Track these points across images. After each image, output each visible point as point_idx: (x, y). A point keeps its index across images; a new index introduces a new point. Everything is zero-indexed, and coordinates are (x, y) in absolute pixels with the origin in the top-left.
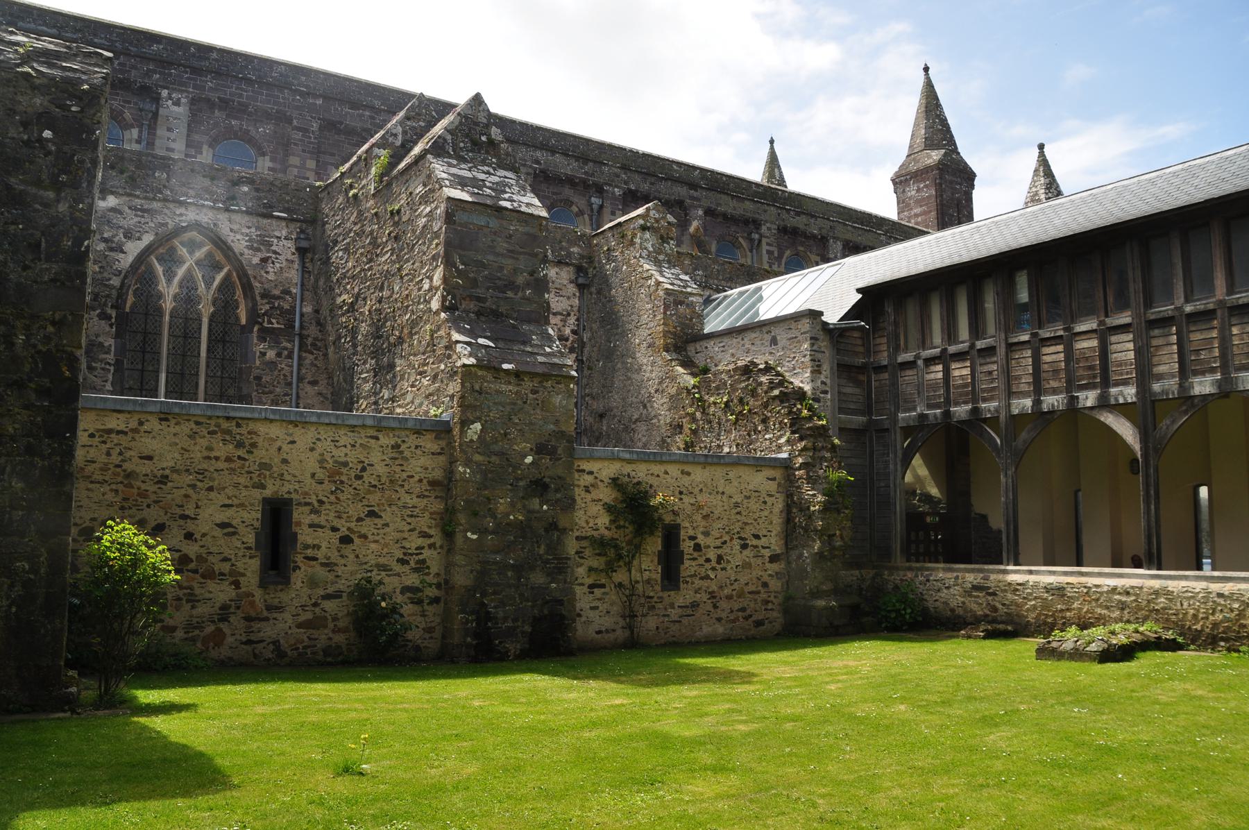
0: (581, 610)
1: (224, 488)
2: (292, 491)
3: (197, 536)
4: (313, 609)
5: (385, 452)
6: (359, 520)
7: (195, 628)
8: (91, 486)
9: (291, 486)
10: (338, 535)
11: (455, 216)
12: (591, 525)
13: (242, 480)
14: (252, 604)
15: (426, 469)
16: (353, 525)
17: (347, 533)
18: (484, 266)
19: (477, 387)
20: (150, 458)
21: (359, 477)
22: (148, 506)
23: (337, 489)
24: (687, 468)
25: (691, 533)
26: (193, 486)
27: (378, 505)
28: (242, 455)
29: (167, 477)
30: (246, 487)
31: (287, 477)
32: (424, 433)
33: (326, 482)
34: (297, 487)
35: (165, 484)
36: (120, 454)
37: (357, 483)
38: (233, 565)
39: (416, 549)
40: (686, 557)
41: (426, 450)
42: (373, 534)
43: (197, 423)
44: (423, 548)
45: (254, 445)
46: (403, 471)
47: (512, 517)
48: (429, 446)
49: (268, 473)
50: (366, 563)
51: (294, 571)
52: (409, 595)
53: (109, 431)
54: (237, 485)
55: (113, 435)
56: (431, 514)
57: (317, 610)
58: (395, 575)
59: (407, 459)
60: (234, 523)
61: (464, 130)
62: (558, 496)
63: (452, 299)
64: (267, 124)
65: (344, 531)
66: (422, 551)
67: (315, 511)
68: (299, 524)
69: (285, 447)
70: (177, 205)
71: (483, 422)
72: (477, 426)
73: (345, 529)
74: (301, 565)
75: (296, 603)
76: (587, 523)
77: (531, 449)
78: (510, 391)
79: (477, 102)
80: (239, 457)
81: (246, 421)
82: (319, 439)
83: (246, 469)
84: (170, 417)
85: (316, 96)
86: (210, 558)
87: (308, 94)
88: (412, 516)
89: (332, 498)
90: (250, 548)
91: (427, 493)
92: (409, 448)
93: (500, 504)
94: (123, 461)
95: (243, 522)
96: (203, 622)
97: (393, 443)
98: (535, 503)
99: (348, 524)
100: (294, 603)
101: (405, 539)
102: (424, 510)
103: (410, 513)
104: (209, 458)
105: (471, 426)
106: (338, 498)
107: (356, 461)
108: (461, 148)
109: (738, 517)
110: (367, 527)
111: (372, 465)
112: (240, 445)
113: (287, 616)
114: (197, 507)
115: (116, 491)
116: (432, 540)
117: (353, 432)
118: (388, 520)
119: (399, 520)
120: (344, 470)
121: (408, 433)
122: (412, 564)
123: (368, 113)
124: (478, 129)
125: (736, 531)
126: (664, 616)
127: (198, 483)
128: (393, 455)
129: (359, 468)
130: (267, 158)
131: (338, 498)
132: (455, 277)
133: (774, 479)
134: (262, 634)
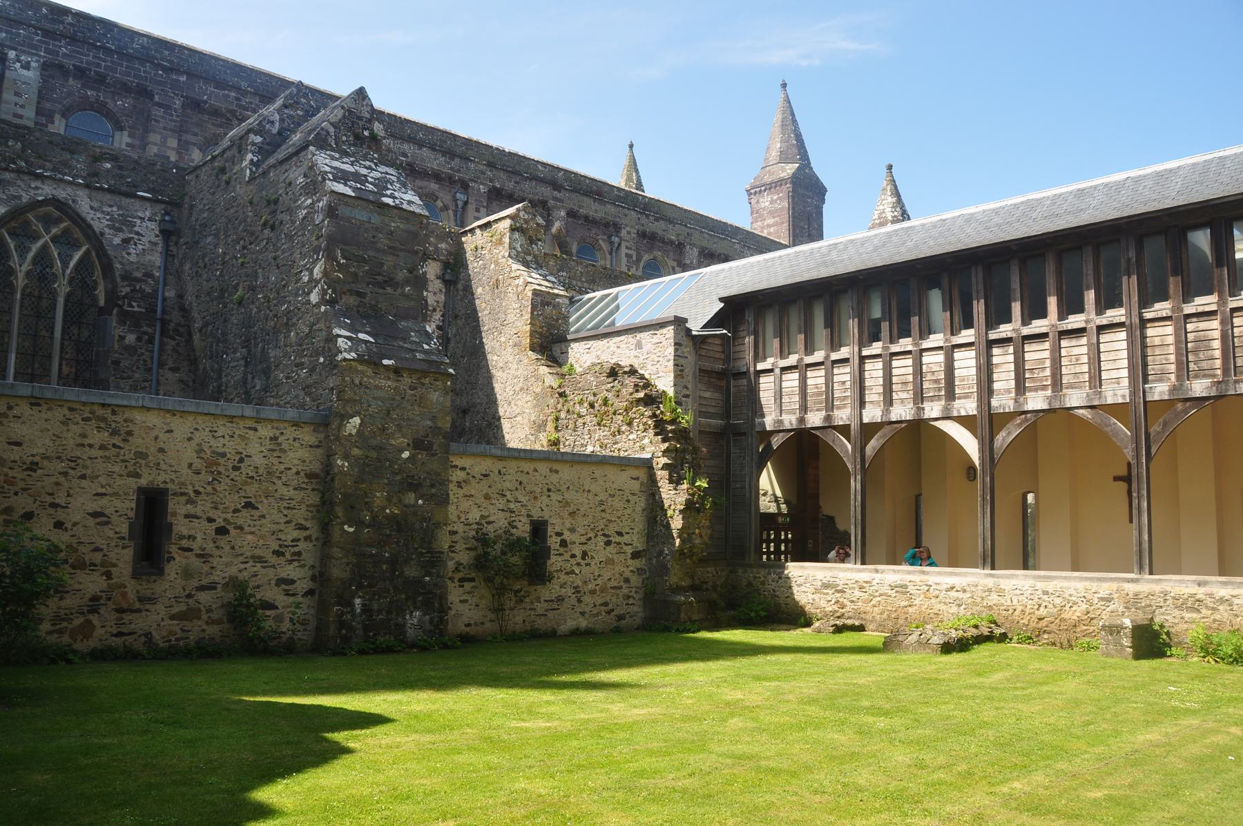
0: (452, 603)
1: (97, 477)
2: (168, 480)
3: (68, 525)
4: (187, 600)
5: (263, 444)
6: (236, 511)
7: (63, 620)
9: (167, 476)
10: (214, 526)
11: (337, 210)
12: (461, 520)
13: (116, 469)
14: (124, 595)
15: (304, 461)
16: (229, 516)
17: (223, 524)
18: (364, 261)
19: (357, 382)
20: (19, 444)
21: (235, 468)
23: (214, 479)
24: (555, 466)
25: (558, 529)
26: (65, 474)
27: (255, 496)
28: (118, 444)
29: (37, 464)
30: (121, 475)
31: (163, 466)
32: (303, 425)
33: (203, 472)
34: (172, 477)
35: (35, 471)
37: (234, 474)
38: (105, 555)
39: (292, 541)
40: (552, 552)
41: (304, 443)
42: (249, 526)
43: (71, 409)
44: (299, 540)
45: (130, 433)
46: (280, 463)
47: (388, 511)
48: (307, 438)
49: (143, 462)
50: (241, 555)
51: (168, 561)
52: (284, 587)
54: (110, 474)
56: (307, 506)
57: (191, 601)
58: (271, 567)
60: (107, 512)
61: (347, 124)
62: (433, 491)
63: (332, 293)
64: (126, 97)
65: (220, 522)
66: (298, 544)
67: (190, 501)
68: (174, 514)
69: (163, 436)
70: (32, 178)
71: (362, 416)
72: (357, 420)
73: (221, 520)
74: (175, 556)
75: (168, 594)
76: (459, 518)
77: (408, 444)
78: (389, 386)
80: (114, 446)
81: (123, 409)
82: (197, 429)
83: (121, 458)
84: (41, 402)
86: (81, 548)
87: (171, 70)
88: (289, 508)
89: (209, 488)
90: (123, 538)
91: (304, 486)
93: (377, 497)
95: (117, 511)
96: (72, 614)
97: (271, 435)
98: (410, 498)
99: (224, 516)
100: (167, 594)
101: (281, 531)
102: (300, 503)
103: (287, 505)
104: (83, 445)
106: (214, 489)
108: (343, 142)
109: (603, 515)
110: (244, 518)
111: (250, 456)
112: (115, 433)
113: (160, 607)
114: (69, 495)
116: (308, 533)
117: (232, 422)
118: (265, 512)
119: (275, 512)
120: (222, 461)
121: (287, 426)
122: (288, 556)
123: (233, 94)
124: (361, 123)
125: (600, 528)
126: (530, 609)
127: (70, 471)
128: (272, 447)
129: (237, 459)
130: (125, 133)
133: (637, 479)
134: (133, 626)
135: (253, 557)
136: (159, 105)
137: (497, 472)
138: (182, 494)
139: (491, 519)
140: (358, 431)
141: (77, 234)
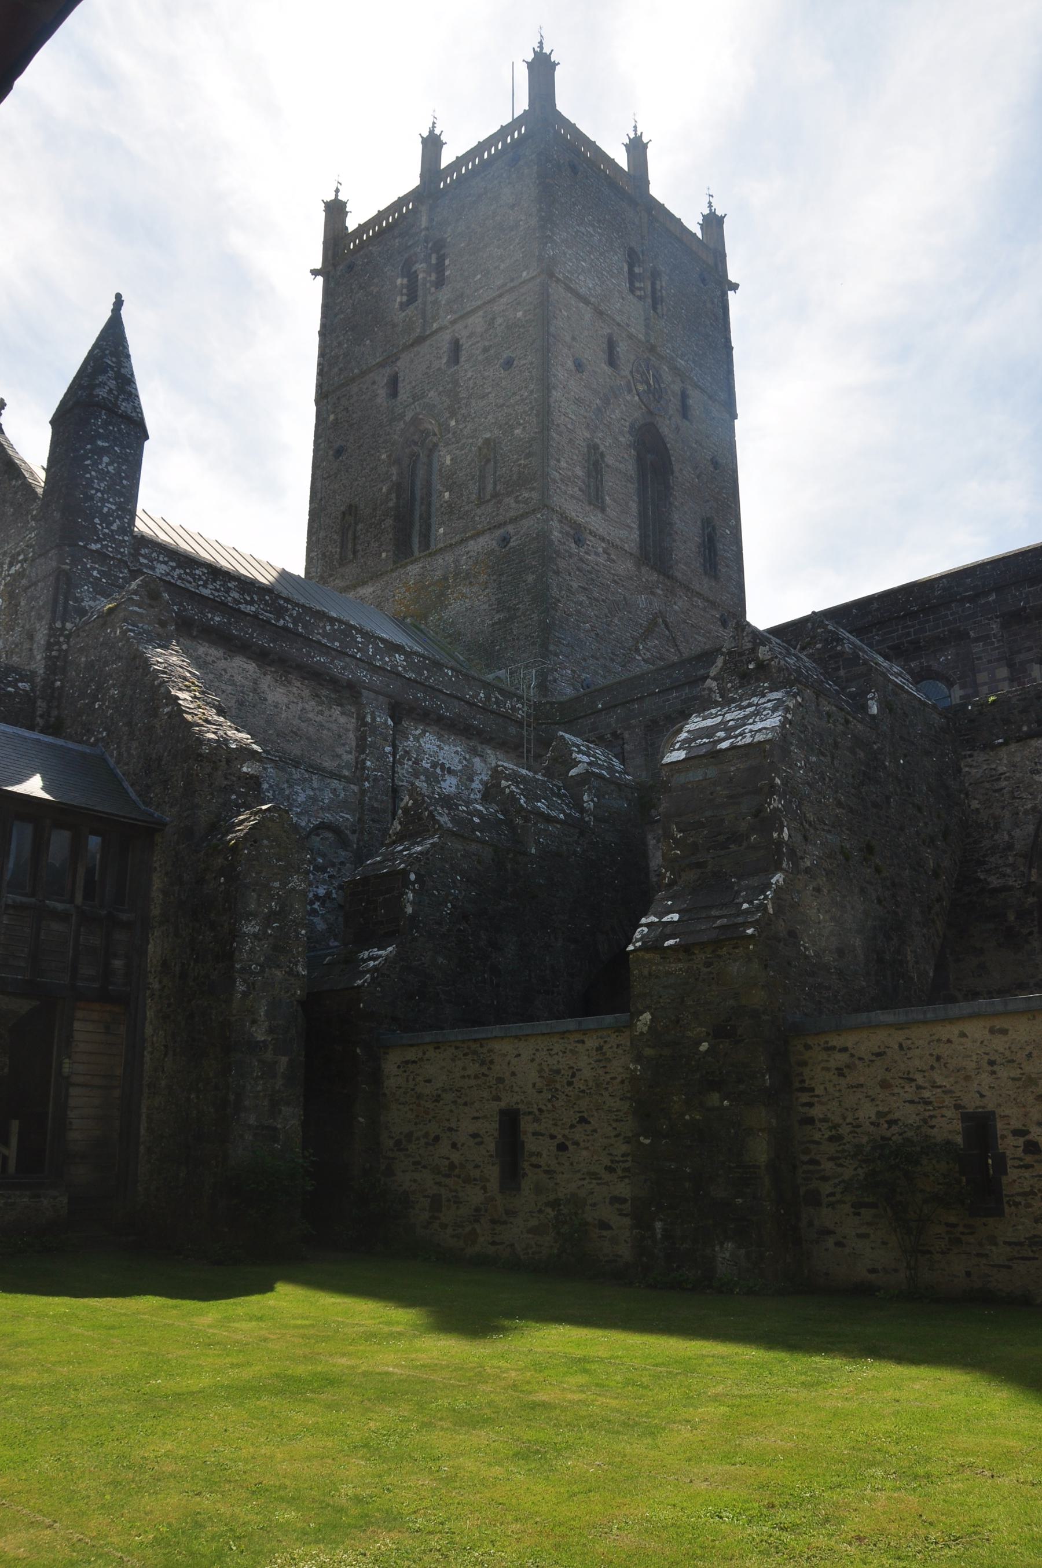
0: (845, 1238)
3: (459, 1145)
6: (572, 1126)
10: (556, 1142)
12: (848, 1120)
13: (485, 1095)
16: (566, 1132)
17: (563, 1140)
20: (429, 1081)
21: (570, 1084)
22: (430, 1121)
23: (553, 1096)
24: (998, 1023)
25: (1016, 1124)
26: (455, 1102)
29: (439, 1096)
30: (488, 1100)
31: (516, 1089)
33: (545, 1091)
34: (523, 1098)
36: (414, 1079)
39: (623, 1156)
40: (1010, 1163)
42: (584, 1141)
43: (457, 1048)
45: (492, 1062)
46: (606, 1073)
47: (687, 1117)
50: (579, 1171)
52: (617, 1206)
53: (407, 1062)
55: (409, 1065)
58: (604, 1184)
59: (609, 1060)
61: (729, 668)
62: (742, 1087)
63: (671, 874)
65: (560, 1138)
67: (537, 1120)
72: (647, 1016)
73: (560, 1137)
77: (708, 1034)
78: (680, 969)
80: (483, 1074)
82: (537, 1050)
88: (617, 1120)
89: (549, 1106)
90: (491, 1156)
92: (611, 1048)
94: (416, 1085)
95: (487, 1132)
97: (597, 1045)
98: (714, 1099)
101: (612, 1145)
103: (615, 1117)
104: (463, 1077)
105: (640, 1018)
106: (553, 1106)
111: (580, 1070)
114: (458, 1121)
115: (412, 1110)
117: (563, 1038)
122: (620, 1173)
124: (744, 658)
126: (978, 1255)
130: (956, 687)
131: (553, 1106)
135: (589, 1173)
136: (977, 640)
137: (896, 1047)
138: (530, 1113)
139: (890, 1117)
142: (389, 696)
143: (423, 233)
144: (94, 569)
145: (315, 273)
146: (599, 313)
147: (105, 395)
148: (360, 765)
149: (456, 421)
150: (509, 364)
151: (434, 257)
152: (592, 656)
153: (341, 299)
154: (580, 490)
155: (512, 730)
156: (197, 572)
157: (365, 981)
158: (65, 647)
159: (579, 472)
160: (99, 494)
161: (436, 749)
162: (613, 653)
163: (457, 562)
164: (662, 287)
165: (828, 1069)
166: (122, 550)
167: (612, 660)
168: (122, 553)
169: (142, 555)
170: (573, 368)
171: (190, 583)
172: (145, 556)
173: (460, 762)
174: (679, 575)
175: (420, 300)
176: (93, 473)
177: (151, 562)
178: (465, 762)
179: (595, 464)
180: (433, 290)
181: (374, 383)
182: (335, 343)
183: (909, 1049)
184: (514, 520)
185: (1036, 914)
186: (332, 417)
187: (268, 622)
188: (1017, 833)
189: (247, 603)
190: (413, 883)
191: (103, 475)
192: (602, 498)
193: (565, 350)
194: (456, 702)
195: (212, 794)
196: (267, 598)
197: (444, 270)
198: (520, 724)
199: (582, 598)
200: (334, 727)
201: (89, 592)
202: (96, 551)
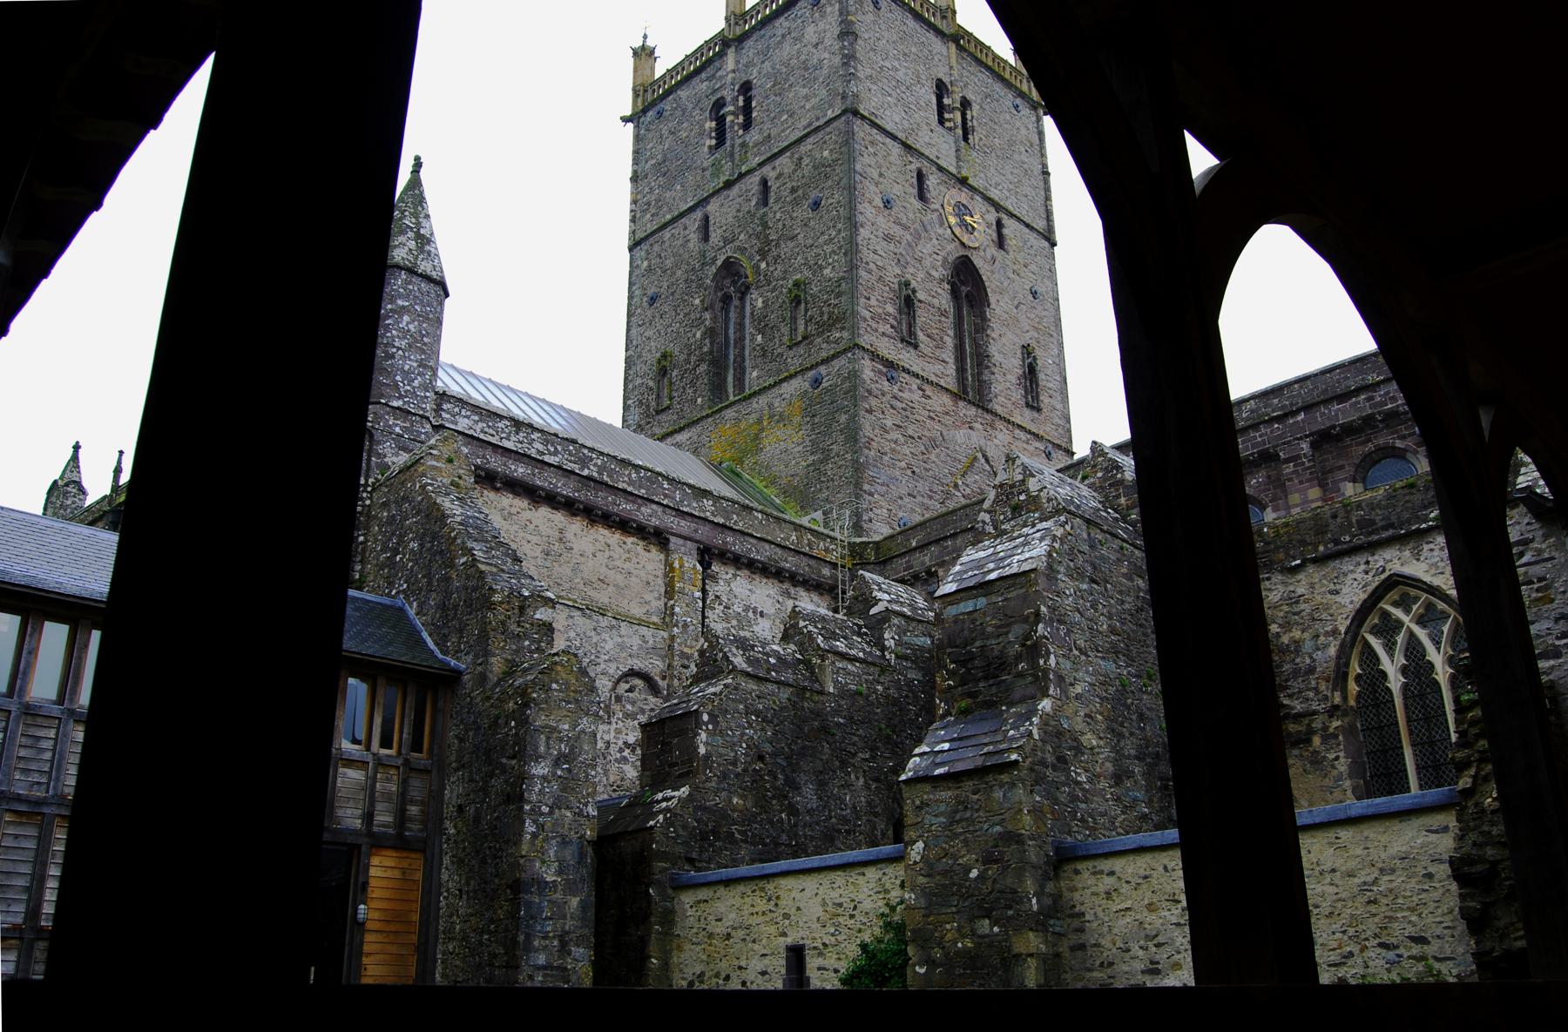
8: (693, 947)
21: (852, 916)
26: (744, 940)
47: (960, 945)
53: (699, 902)
64: (1258, 472)
67: (821, 954)
72: (920, 845)
79: (1010, 462)
85: (1294, 413)
87: (1286, 416)
89: (833, 939)
107: (848, 901)
109: (1373, 908)
124: (1015, 490)
125: (1369, 933)
130: (1269, 510)
132: (948, 680)
133: (1445, 829)
136: (1287, 461)
138: (815, 948)
139: (1160, 939)
140: (922, 857)
141: (1374, 619)
142: (697, 542)
143: (730, 76)
144: (397, 425)
145: (625, 120)
146: (907, 147)
147: (405, 256)
148: (668, 612)
149: (768, 264)
150: (816, 205)
151: (741, 98)
152: (909, 495)
153: (651, 145)
154: (892, 327)
155: (826, 571)
156: (500, 425)
157: (658, 822)
158: (368, 502)
159: (890, 309)
160: (400, 352)
161: (748, 593)
162: (931, 491)
163: (770, 406)
164: (972, 117)
165: (1095, 894)
166: (424, 406)
167: (931, 498)
168: (423, 409)
169: (444, 410)
170: (881, 205)
171: (493, 436)
172: (447, 412)
173: (773, 604)
174: (999, 410)
175: (728, 143)
176: (394, 332)
177: (454, 416)
178: (778, 606)
179: (908, 303)
180: (741, 132)
181: (685, 228)
182: (647, 190)
183: (1174, 870)
184: (826, 361)
185: (1341, 738)
186: (646, 264)
187: (572, 472)
188: (1318, 655)
189: (550, 454)
190: (706, 724)
191: (405, 333)
192: (915, 334)
193: (873, 188)
194: (767, 546)
195: (505, 641)
196: (571, 448)
197: (751, 112)
198: (834, 565)
199: (895, 435)
200: (642, 573)
201: (392, 448)
202: (398, 408)
